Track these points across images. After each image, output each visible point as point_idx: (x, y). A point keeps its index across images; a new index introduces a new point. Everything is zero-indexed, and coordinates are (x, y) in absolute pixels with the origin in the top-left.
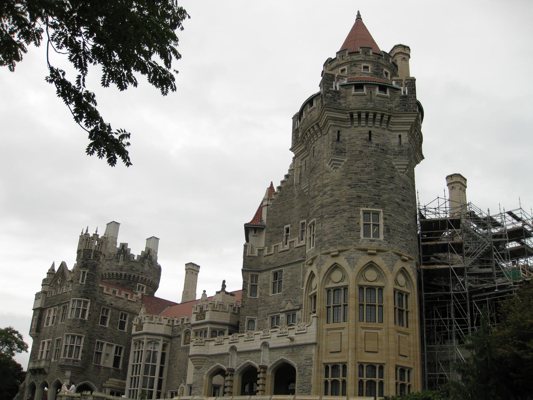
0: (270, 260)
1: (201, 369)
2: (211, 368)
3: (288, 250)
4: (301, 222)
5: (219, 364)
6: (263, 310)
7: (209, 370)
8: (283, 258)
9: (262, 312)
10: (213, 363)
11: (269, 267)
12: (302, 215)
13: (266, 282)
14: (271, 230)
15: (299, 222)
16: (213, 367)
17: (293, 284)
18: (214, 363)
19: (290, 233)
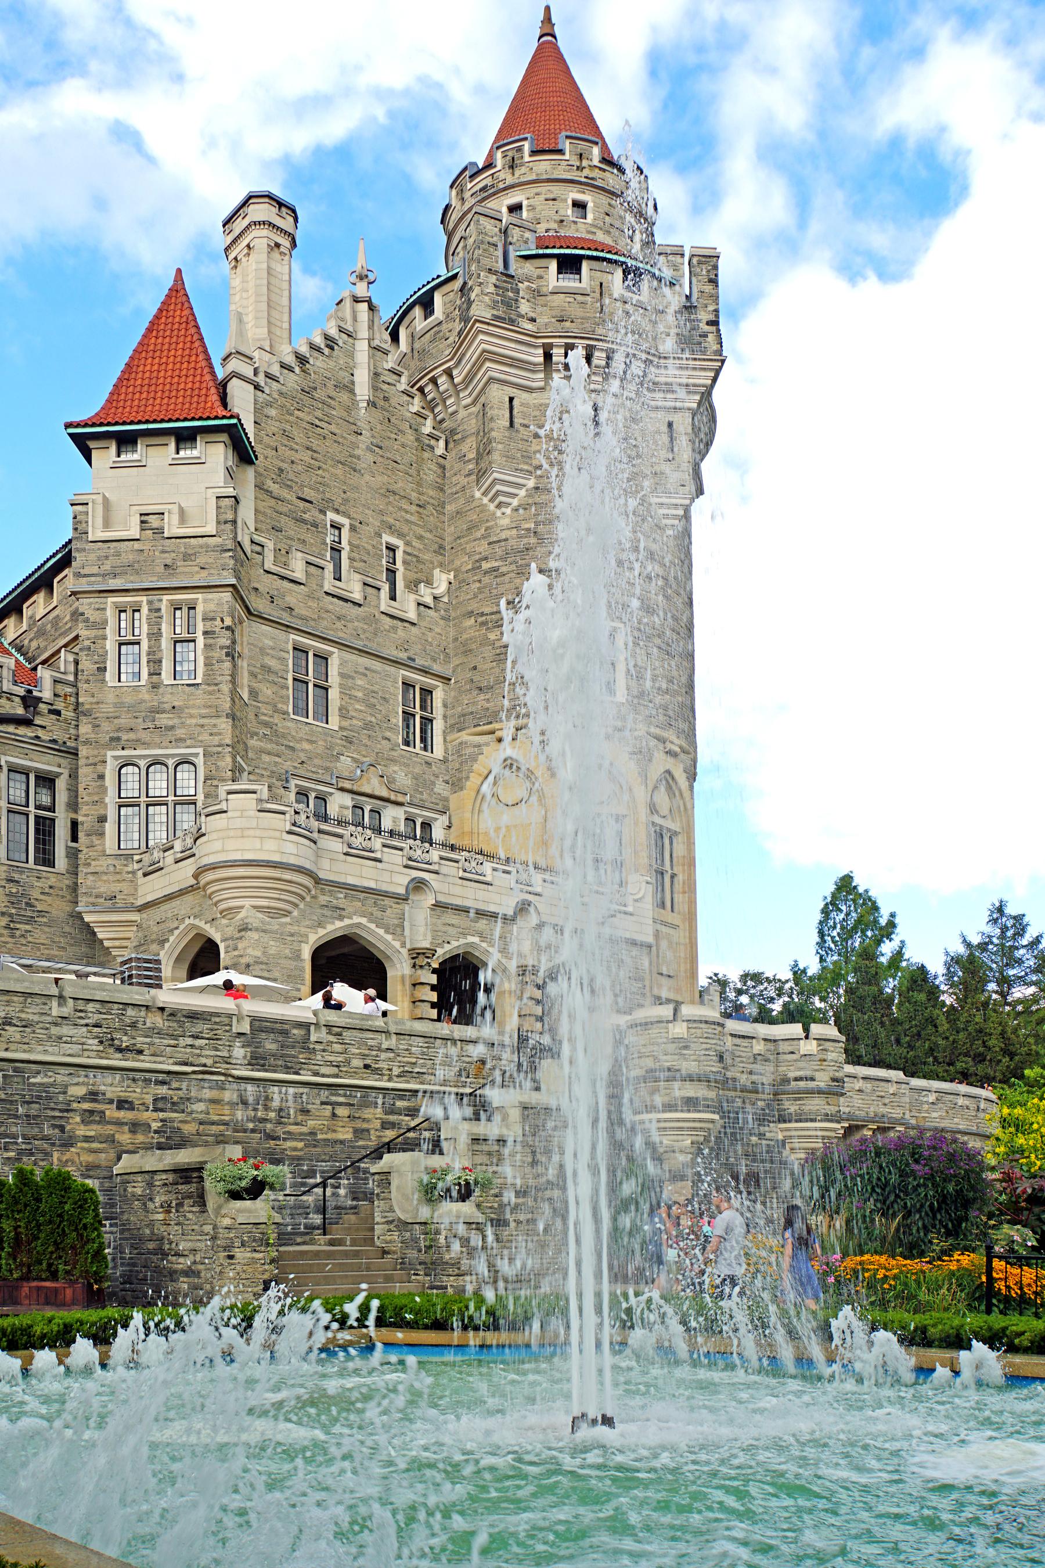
0: (291, 600)
1: (287, 920)
2: (330, 928)
3: (360, 605)
4: (387, 538)
5: (364, 921)
6: (269, 753)
7: (322, 932)
8: (339, 618)
9: (266, 758)
10: (339, 912)
11: (286, 618)
12: (391, 521)
13: (272, 663)
14: (274, 488)
15: (380, 536)
16: (339, 924)
17: (373, 719)
18: (343, 913)
19: (352, 551)
